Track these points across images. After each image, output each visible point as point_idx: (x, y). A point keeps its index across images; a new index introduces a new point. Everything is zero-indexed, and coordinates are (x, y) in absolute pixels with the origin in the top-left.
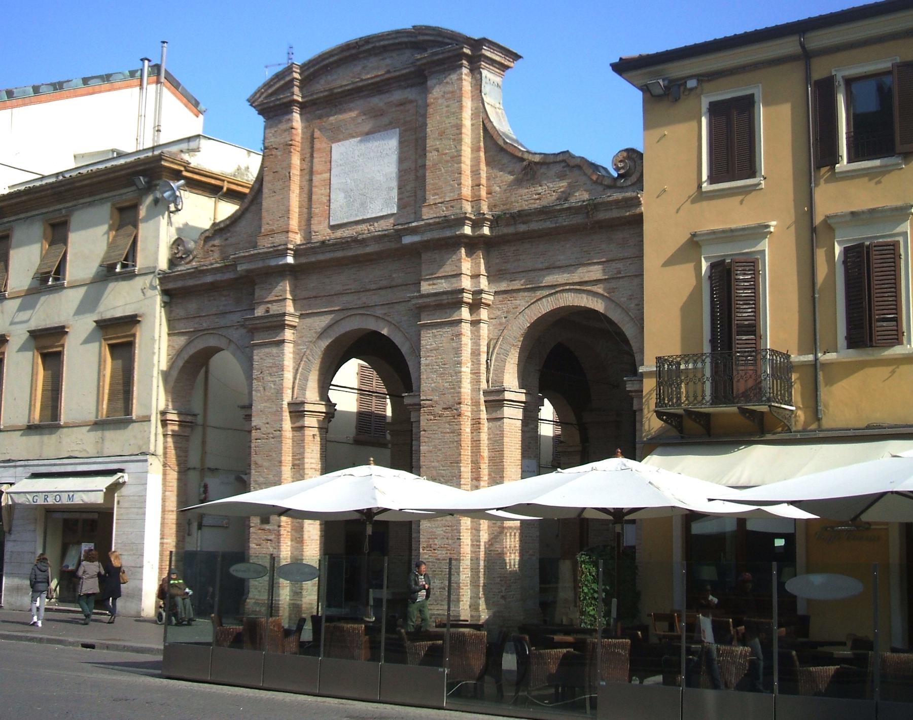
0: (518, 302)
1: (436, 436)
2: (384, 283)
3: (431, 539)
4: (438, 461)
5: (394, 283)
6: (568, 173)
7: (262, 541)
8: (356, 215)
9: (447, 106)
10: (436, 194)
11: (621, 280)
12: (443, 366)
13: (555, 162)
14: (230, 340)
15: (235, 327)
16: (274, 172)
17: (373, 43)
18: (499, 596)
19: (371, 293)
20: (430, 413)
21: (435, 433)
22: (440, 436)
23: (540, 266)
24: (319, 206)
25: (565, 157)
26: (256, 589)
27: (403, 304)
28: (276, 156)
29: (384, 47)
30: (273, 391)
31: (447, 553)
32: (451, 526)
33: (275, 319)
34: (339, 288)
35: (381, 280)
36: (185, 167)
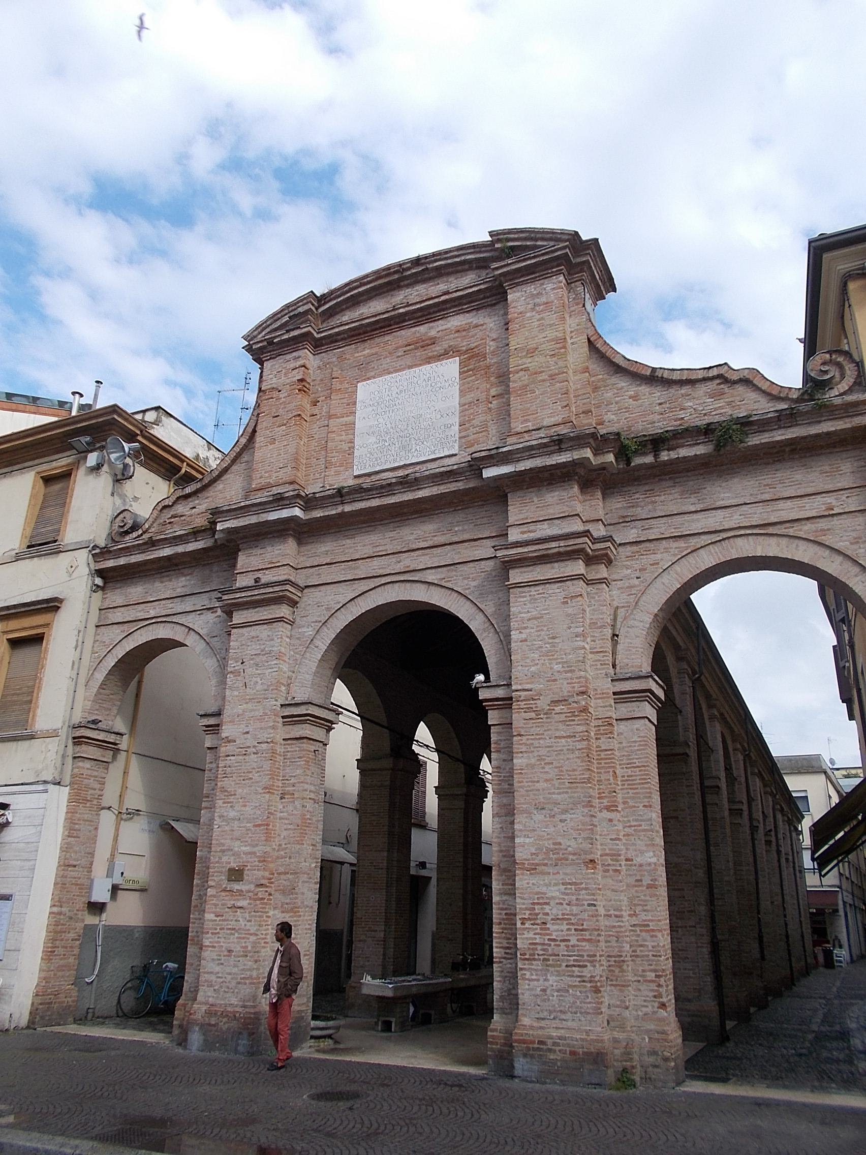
0: (659, 556)
1: (541, 742)
3: (538, 904)
4: (546, 780)
6: (726, 390)
7: (227, 910)
8: (395, 461)
11: (835, 518)
12: (550, 641)
13: (705, 379)
14: (190, 629)
15: (199, 612)
16: (274, 417)
17: (423, 264)
18: (656, 1005)
20: (529, 710)
21: (539, 739)
22: (548, 742)
23: (693, 509)
24: (337, 454)
25: (722, 371)
26: (211, 986)
27: (471, 564)
28: (278, 399)
29: (437, 268)
30: (259, 687)
31: (568, 930)
32: (575, 884)
33: (271, 590)
34: (368, 551)
35: (435, 536)
36: (141, 432)
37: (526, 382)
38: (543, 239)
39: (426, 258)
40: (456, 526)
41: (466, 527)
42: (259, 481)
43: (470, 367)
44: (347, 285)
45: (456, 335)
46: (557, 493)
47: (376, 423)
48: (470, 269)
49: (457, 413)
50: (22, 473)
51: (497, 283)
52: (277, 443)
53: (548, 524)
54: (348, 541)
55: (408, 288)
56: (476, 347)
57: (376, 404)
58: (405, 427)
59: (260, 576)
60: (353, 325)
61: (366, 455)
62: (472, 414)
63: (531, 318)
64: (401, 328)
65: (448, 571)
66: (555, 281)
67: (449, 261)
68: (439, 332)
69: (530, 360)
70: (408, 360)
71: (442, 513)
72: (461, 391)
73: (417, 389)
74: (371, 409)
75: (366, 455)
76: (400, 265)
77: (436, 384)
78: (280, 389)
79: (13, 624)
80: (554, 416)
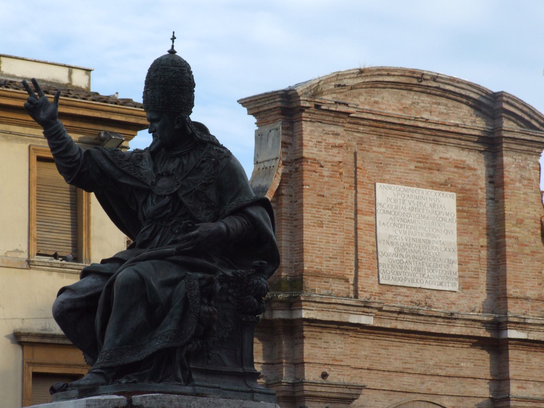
2: (451, 371)
5: (462, 374)
9: (525, 194)
10: (516, 287)
19: (437, 378)
28: (322, 176)
34: (397, 365)
35: (448, 367)
37: (516, 251)
38: (537, 121)
39: (441, 78)
40: (462, 362)
41: (469, 365)
42: (310, 264)
43: (465, 209)
44: (379, 69)
45: (456, 170)
46: (538, 360)
47: (394, 234)
48: (467, 104)
49: (456, 250)
50: (8, 140)
51: (492, 136)
52: (325, 228)
53: (533, 384)
54: (383, 352)
55: (415, 94)
56: (470, 190)
57: (393, 213)
58: (418, 249)
59: (326, 370)
60: (379, 118)
61: (388, 266)
62: (467, 257)
63: (519, 189)
64: (412, 138)
65: (458, 401)
66: (535, 160)
67: (457, 90)
68: (441, 158)
69: (518, 230)
70: (415, 177)
71: (453, 347)
72: (458, 229)
73: (425, 211)
74: (389, 216)
75: (388, 266)
76: (423, 74)
77: (439, 214)
78: (322, 163)
79: (41, 355)
80: (533, 290)
